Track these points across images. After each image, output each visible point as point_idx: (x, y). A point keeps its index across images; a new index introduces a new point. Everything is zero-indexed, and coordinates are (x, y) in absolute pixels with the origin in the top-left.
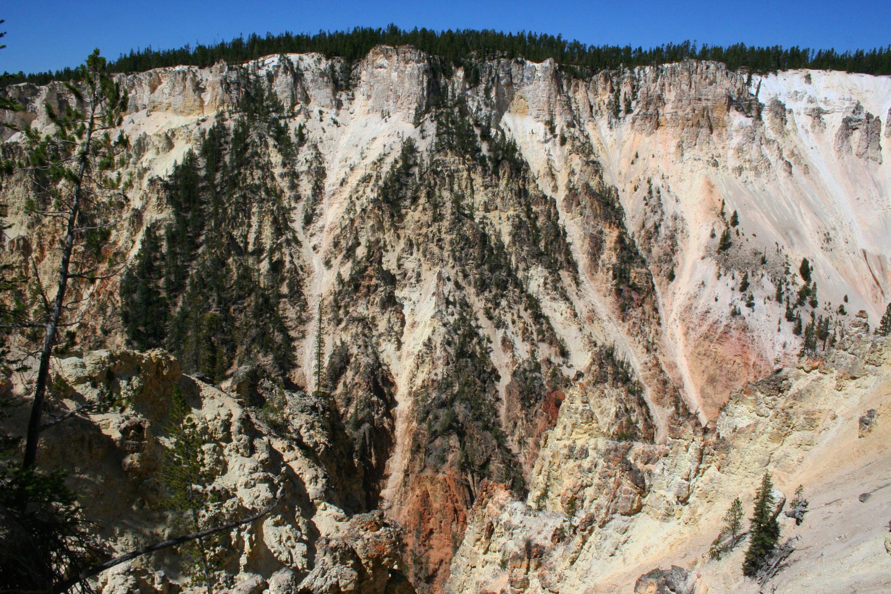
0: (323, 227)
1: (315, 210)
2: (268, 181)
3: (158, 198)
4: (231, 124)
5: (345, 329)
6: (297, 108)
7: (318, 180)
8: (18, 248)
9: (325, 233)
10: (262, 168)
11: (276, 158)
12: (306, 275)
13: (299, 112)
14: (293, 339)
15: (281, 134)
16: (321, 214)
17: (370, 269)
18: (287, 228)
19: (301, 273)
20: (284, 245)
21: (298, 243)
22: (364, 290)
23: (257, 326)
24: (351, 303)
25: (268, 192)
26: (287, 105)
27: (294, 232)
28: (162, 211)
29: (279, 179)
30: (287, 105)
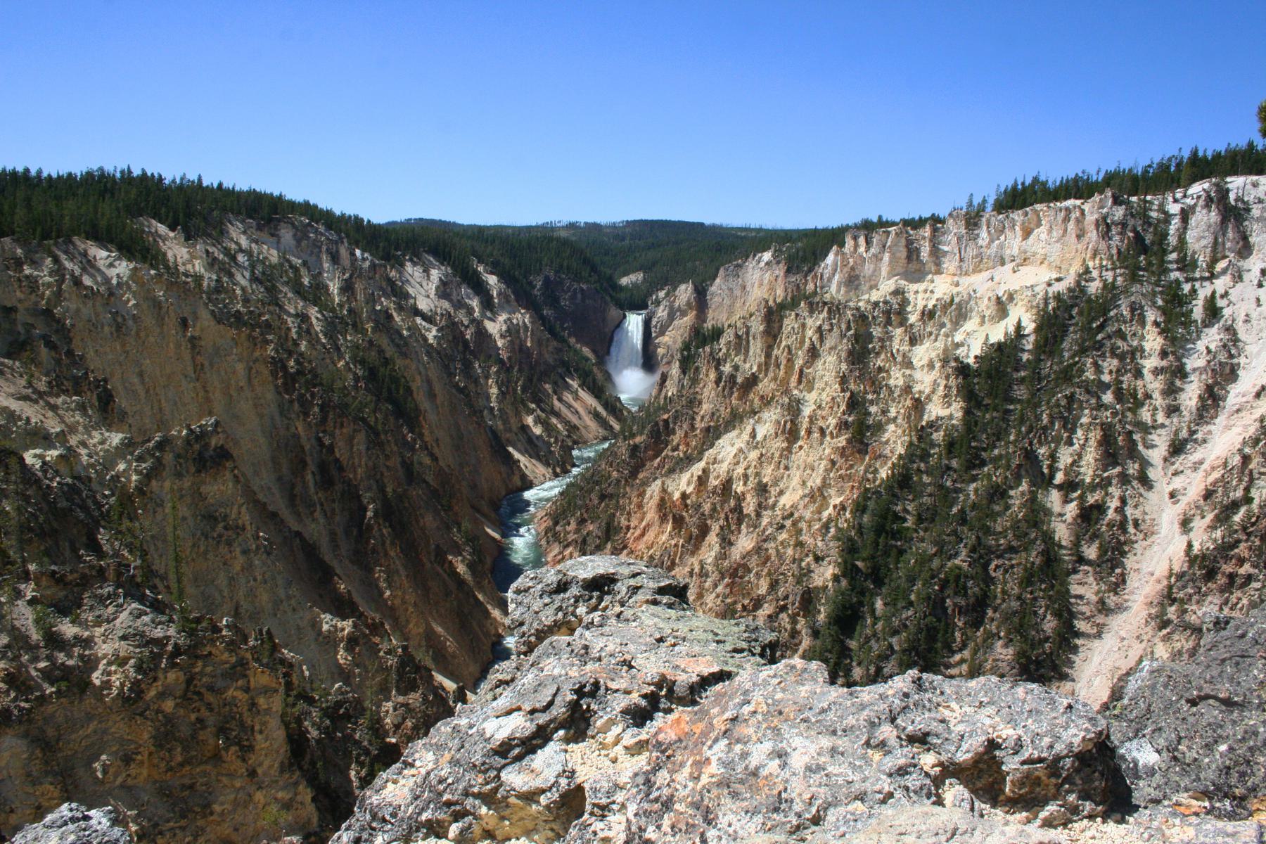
0: (1201, 463)
1: (1195, 432)
2: (1126, 378)
3: (946, 386)
4: (1094, 287)
5: (1166, 639)
6: (1221, 265)
7: (1216, 383)
8: (784, 432)
9: (1201, 473)
10: (1121, 357)
11: (1153, 341)
12: (1141, 536)
13: (1224, 272)
14: (1078, 634)
15: (1175, 304)
16: (1205, 441)
17: (1242, 545)
18: (1133, 453)
19: (1131, 530)
20: (1114, 481)
21: (1145, 481)
22: (1221, 580)
23: (1019, 598)
24: (1195, 598)
25: (1119, 394)
26: (1202, 260)
27: (1145, 464)
28: (950, 405)
29: (1148, 376)
30: (1202, 260)
